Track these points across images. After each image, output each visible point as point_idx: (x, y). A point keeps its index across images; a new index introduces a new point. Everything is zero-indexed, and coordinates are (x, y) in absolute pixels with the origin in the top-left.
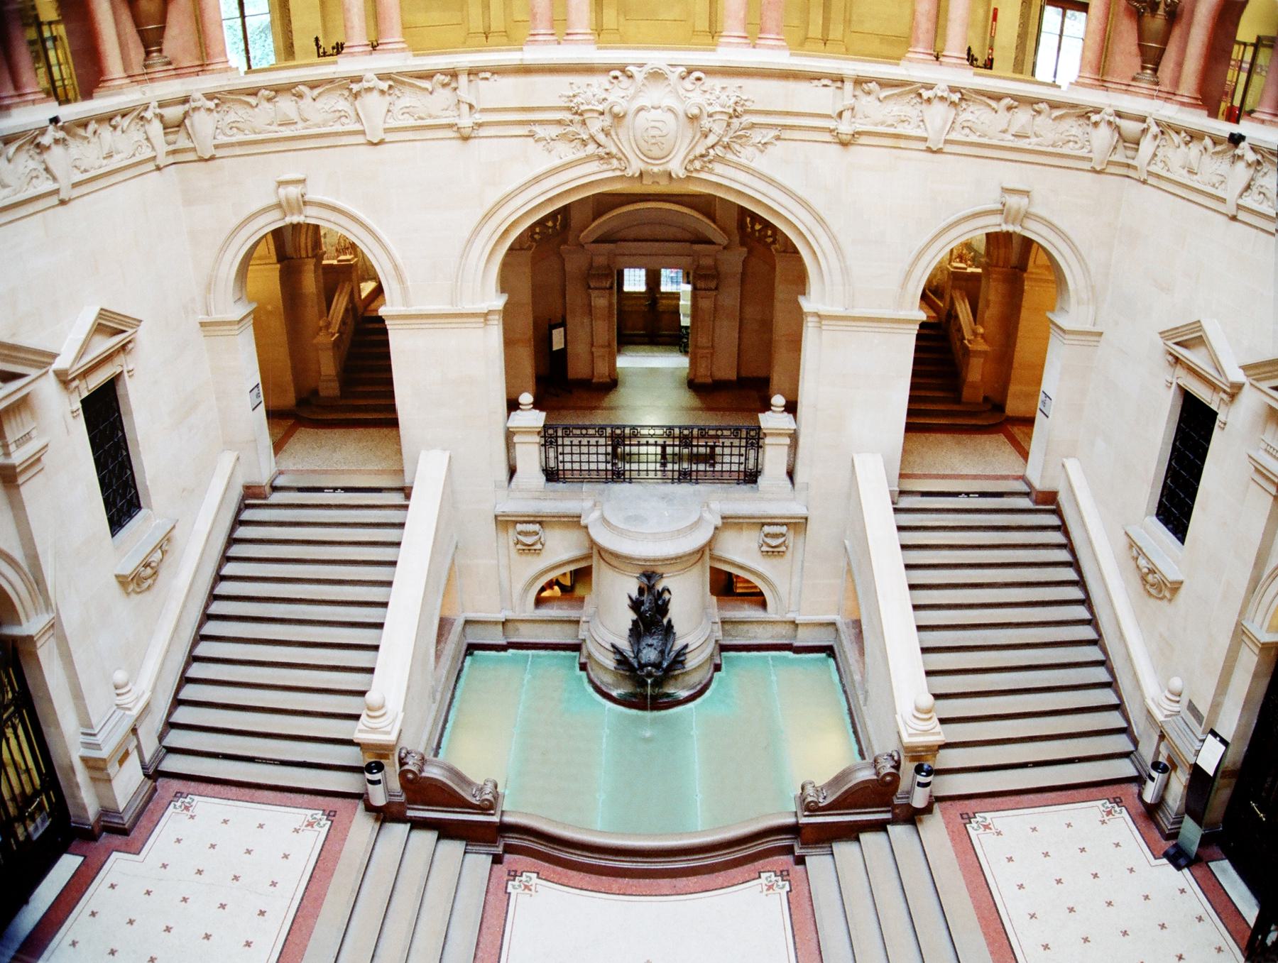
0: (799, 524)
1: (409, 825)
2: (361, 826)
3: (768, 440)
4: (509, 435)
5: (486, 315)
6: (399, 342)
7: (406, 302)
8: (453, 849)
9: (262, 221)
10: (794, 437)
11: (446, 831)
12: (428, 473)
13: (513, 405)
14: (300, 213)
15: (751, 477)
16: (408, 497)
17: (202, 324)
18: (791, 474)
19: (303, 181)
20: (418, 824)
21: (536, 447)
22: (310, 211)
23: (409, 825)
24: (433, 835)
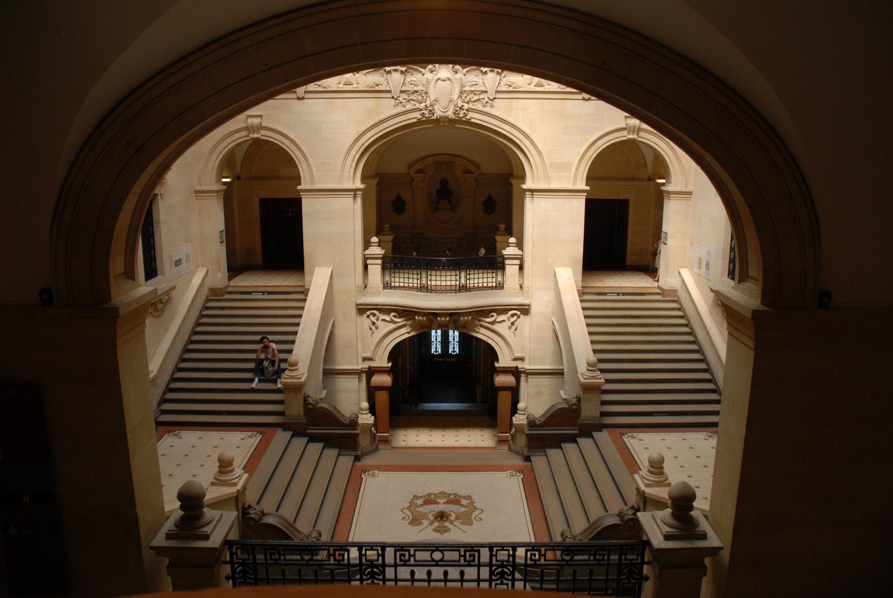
0: (525, 310)
1: (307, 439)
2: (282, 437)
3: (507, 262)
4: (365, 259)
5: (355, 191)
6: (308, 205)
7: (313, 183)
8: (332, 453)
9: (237, 136)
10: (521, 259)
11: (329, 442)
12: (318, 279)
13: (367, 244)
14: (258, 133)
15: (500, 286)
16: (307, 295)
17: (196, 192)
18: (521, 287)
19: (261, 116)
20: (313, 439)
21: (379, 267)
22: (263, 132)
23: (307, 439)
24: (320, 445)
